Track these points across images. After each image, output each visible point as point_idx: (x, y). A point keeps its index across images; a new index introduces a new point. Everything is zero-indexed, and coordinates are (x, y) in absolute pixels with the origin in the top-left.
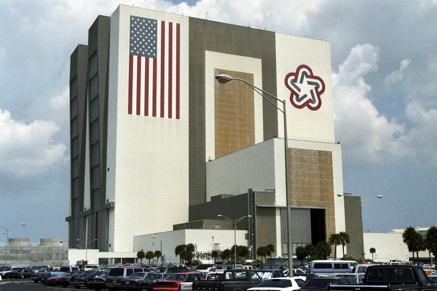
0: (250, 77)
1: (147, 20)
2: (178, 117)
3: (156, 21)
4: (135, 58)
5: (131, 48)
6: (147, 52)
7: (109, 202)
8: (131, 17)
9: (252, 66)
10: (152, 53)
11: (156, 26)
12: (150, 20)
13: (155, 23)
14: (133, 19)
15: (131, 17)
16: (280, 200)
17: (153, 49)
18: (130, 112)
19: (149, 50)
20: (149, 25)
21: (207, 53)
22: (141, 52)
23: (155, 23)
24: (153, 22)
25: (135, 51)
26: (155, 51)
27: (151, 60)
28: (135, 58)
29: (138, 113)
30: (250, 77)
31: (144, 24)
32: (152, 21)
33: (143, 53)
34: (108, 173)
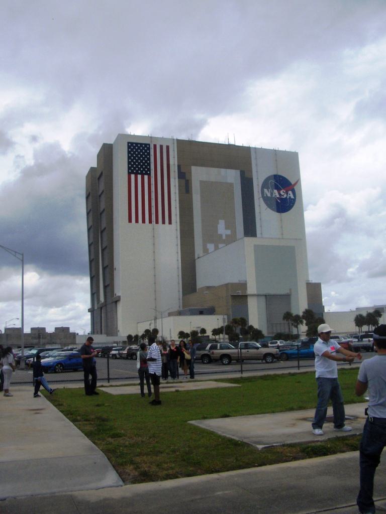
0: (231, 185)
2: (170, 223)
3: (149, 145)
4: (133, 176)
5: (129, 168)
6: (142, 171)
7: (117, 295)
8: (128, 143)
9: (232, 176)
10: (147, 171)
11: (149, 149)
12: (144, 144)
13: (148, 146)
14: (130, 144)
15: (128, 143)
16: (252, 289)
17: (147, 168)
18: (130, 221)
20: (143, 148)
21: (193, 168)
22: (137, 171)
23: (148, 146)
24: (147, 146)
25: (132, 171)
27: (146, 177)
28: (133, 176)
29: (137, 221)
31: (139, 148)
32: (146, 145)
33: (139, 172)
34: (115, 273)
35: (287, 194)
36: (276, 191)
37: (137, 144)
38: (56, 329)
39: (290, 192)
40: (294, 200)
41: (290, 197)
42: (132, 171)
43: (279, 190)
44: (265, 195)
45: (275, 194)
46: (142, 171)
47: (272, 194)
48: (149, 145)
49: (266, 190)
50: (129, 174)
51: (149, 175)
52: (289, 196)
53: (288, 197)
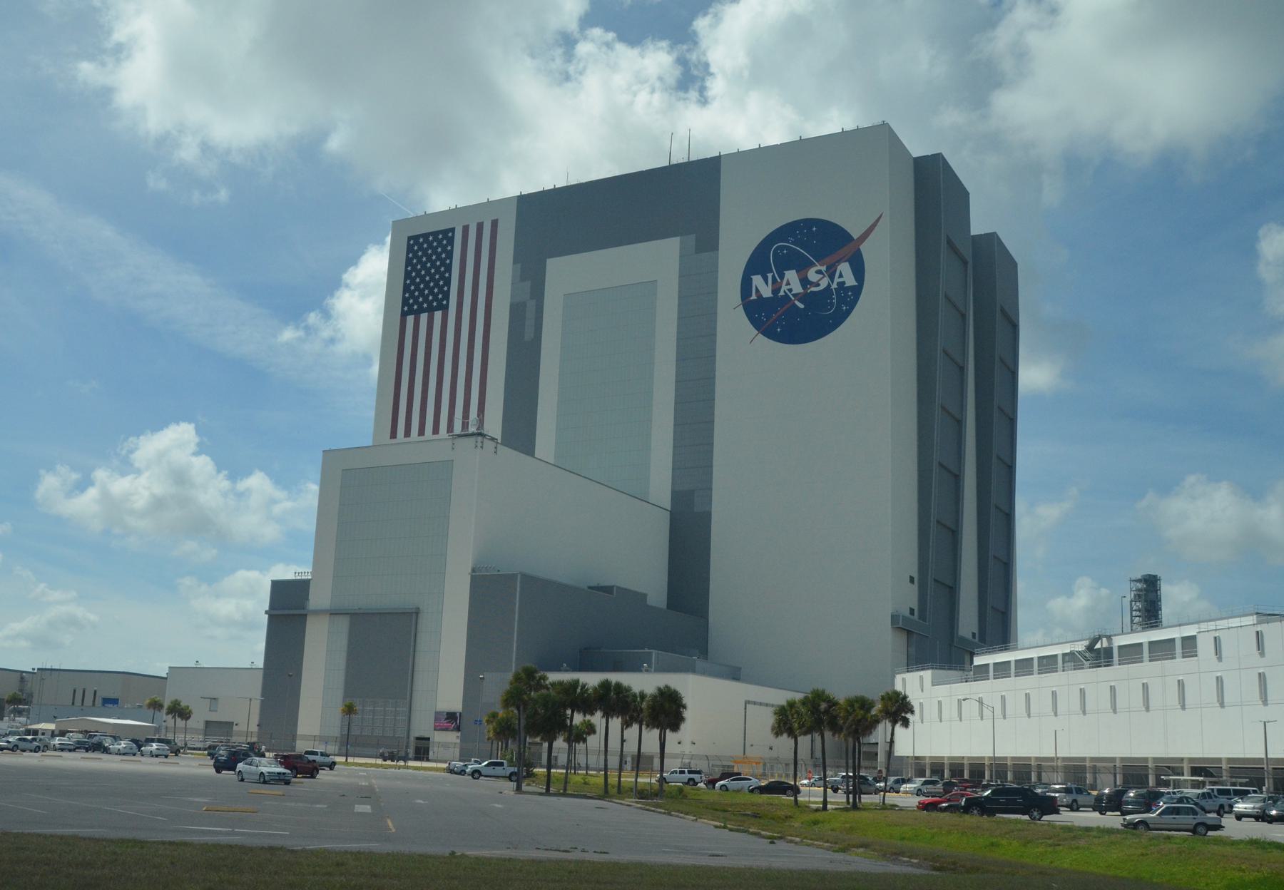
1: (435, 234)
3: (453, 230)
4: (410, 319)
5: (405, 302)
8: (409, 239)
15: (409, 239)
18: (394, 434)
19: (436, 299)
20: (440, 242)
21: (550, 262)
24: (448, 234)
26: (447, 296)
28: (410, 319)
32: (445, 232)
35: (832, 277)
36: (791, 275)
37: (426, 236)
39: (845, 269)
40: (857, 291)
41: (841, 284)
42: (411, 306)
43: (802, 266)
44: (754, 297)
45: (788, 284)
46: (430, 304)
48: (453, 230)
49: (757, 280)
50: (404, 315)
51: (445, 309)
52: (837, 280)
53: (834, 286)
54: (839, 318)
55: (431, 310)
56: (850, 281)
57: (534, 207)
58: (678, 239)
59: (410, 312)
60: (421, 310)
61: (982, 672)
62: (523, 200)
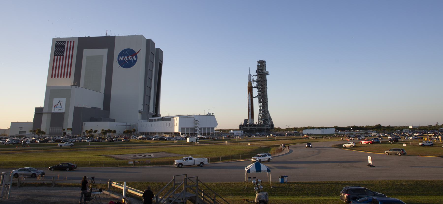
0: (102, 56)
4: (56, 57)
5: (55, 53)
9: (104, 52)
11: (65, 43)
24: (64, 42)
26: (64, 53)
27: (62, 57)
28: (56, 57)
30: (102, 56)
32: (64, 42)
36: (126, 57)
37: (60, 42)
38: (13, 124)
39: (134, 57)
40: (136, 61)
47: (123, 59)
49: (120, 57)
50: (55, 56)
51: (63, 56)
54: (133, 65)
55: (60, 56)
56: (135, 59)
57: (81, 40)
58: (107, 49)
59: (56, 55)
60: (58, 55)
61: (150, 121)
62: (79, 38)
